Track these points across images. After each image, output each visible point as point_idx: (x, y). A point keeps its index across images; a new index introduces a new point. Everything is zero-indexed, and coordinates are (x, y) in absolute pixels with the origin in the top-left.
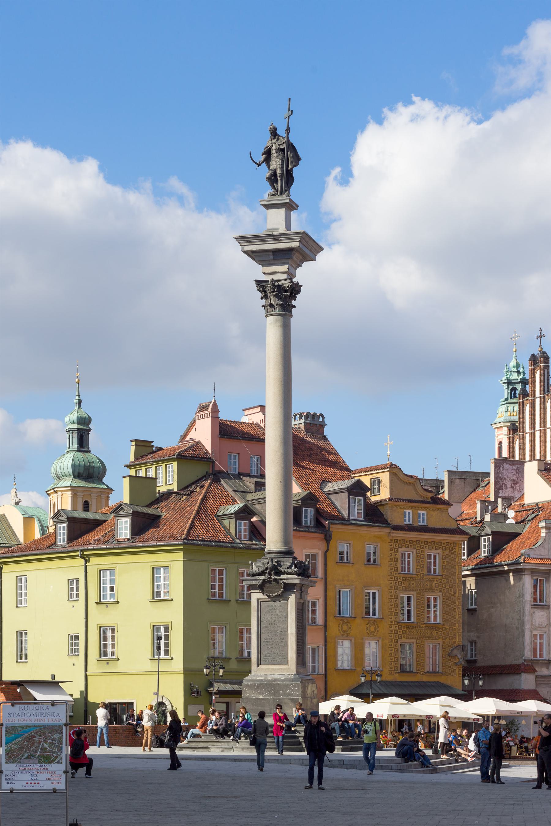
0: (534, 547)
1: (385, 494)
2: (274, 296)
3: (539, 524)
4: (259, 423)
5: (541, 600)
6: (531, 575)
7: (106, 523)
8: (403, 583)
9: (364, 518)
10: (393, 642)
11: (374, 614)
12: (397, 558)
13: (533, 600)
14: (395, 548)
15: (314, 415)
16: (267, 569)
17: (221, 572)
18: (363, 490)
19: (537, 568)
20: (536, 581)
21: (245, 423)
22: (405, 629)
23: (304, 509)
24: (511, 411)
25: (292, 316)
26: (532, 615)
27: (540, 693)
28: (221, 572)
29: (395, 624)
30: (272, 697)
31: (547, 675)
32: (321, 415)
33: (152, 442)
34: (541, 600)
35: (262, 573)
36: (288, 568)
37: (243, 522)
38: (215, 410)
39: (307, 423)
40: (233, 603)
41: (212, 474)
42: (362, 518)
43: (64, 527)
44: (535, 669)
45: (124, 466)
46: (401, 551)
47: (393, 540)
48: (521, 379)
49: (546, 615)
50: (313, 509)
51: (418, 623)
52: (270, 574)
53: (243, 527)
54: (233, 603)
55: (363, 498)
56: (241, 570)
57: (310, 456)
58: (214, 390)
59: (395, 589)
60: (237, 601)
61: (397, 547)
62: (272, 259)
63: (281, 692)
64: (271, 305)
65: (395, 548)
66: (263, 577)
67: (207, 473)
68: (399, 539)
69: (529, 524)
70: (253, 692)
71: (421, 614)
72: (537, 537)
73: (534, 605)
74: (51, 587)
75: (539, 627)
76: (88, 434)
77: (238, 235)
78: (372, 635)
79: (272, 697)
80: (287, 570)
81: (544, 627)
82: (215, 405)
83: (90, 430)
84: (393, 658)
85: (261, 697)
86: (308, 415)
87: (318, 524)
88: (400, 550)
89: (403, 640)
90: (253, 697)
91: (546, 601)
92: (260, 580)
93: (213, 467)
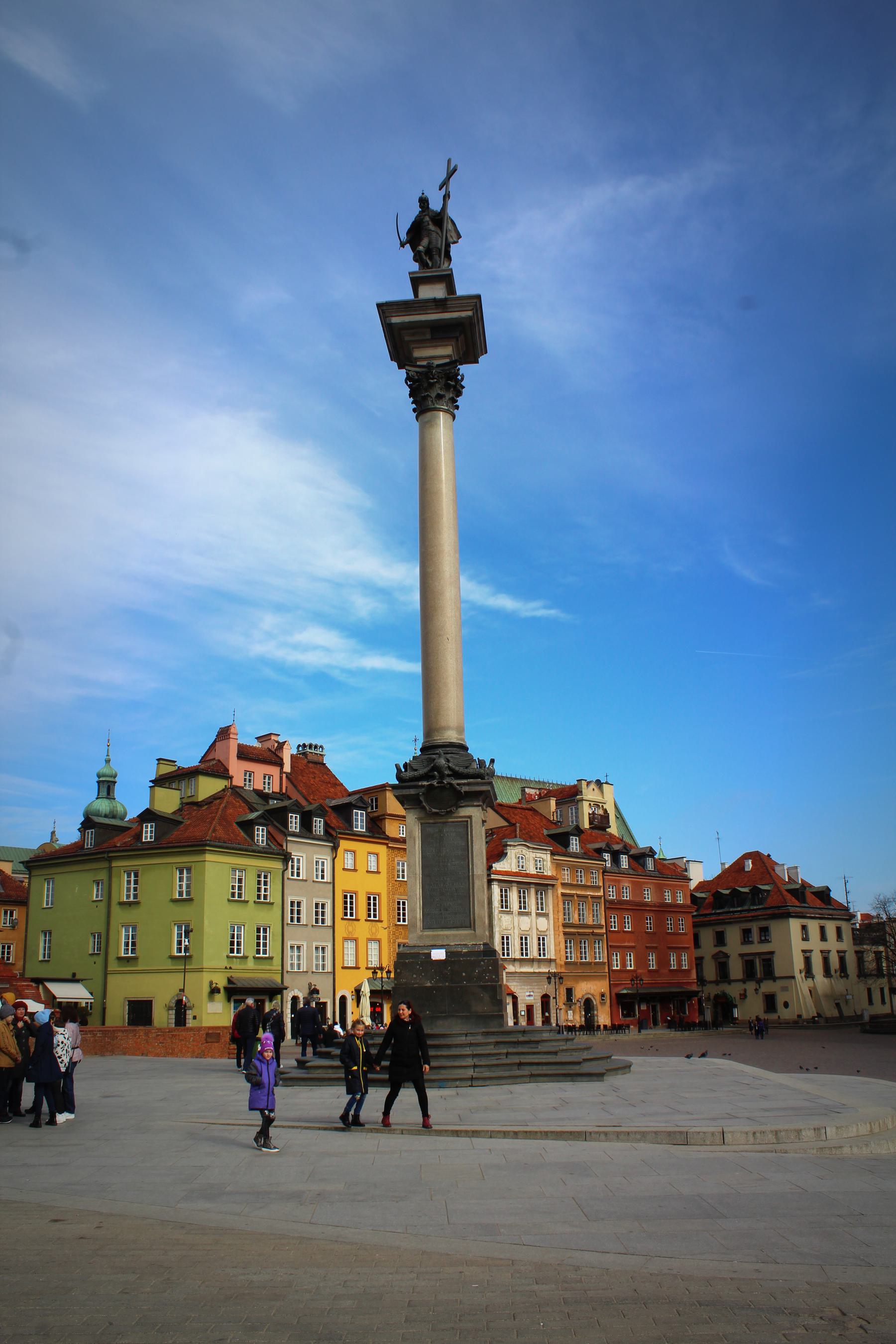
7: (131, 830)
10: (392, 942)
12: (394, 867)
13: (500, 906)
14: (392, 858)
15: (316, 747)
18: (364, 804)
19: (503, 879)
20: (501, 891)
22: (401, 930)
23: (314, 819)
26: (500, 919)
27: (510, 987)
30: (447, 984)
31: (514, 971)
32: (321, 747)
33: (176, 762)
36: (467, 767)
40: (251, 903)
41: (230, 788)
42: (364, 830)
43: (92, 832)
44: (505, 967)
45: (150, 781)
50: (322, 820)
54: (251, 903)
57: (314, 778)
60: (255, 902)
62: (428, 336)
63: (464, 974)
65: (392, 858)
66: (425, 783)
67: (226, 786)
70: (415, 976)
73: (501, 911)
74: (77, 888)
75: (505, 930)
76: (114, 785)
79: (447, 984)
80: (466, 771)
83: (115, 782)
84: (392, 957)
85: (429, 984)
88: (396, 860)
89: (400, 940)
90: (415, 984)
92: (423, 786)
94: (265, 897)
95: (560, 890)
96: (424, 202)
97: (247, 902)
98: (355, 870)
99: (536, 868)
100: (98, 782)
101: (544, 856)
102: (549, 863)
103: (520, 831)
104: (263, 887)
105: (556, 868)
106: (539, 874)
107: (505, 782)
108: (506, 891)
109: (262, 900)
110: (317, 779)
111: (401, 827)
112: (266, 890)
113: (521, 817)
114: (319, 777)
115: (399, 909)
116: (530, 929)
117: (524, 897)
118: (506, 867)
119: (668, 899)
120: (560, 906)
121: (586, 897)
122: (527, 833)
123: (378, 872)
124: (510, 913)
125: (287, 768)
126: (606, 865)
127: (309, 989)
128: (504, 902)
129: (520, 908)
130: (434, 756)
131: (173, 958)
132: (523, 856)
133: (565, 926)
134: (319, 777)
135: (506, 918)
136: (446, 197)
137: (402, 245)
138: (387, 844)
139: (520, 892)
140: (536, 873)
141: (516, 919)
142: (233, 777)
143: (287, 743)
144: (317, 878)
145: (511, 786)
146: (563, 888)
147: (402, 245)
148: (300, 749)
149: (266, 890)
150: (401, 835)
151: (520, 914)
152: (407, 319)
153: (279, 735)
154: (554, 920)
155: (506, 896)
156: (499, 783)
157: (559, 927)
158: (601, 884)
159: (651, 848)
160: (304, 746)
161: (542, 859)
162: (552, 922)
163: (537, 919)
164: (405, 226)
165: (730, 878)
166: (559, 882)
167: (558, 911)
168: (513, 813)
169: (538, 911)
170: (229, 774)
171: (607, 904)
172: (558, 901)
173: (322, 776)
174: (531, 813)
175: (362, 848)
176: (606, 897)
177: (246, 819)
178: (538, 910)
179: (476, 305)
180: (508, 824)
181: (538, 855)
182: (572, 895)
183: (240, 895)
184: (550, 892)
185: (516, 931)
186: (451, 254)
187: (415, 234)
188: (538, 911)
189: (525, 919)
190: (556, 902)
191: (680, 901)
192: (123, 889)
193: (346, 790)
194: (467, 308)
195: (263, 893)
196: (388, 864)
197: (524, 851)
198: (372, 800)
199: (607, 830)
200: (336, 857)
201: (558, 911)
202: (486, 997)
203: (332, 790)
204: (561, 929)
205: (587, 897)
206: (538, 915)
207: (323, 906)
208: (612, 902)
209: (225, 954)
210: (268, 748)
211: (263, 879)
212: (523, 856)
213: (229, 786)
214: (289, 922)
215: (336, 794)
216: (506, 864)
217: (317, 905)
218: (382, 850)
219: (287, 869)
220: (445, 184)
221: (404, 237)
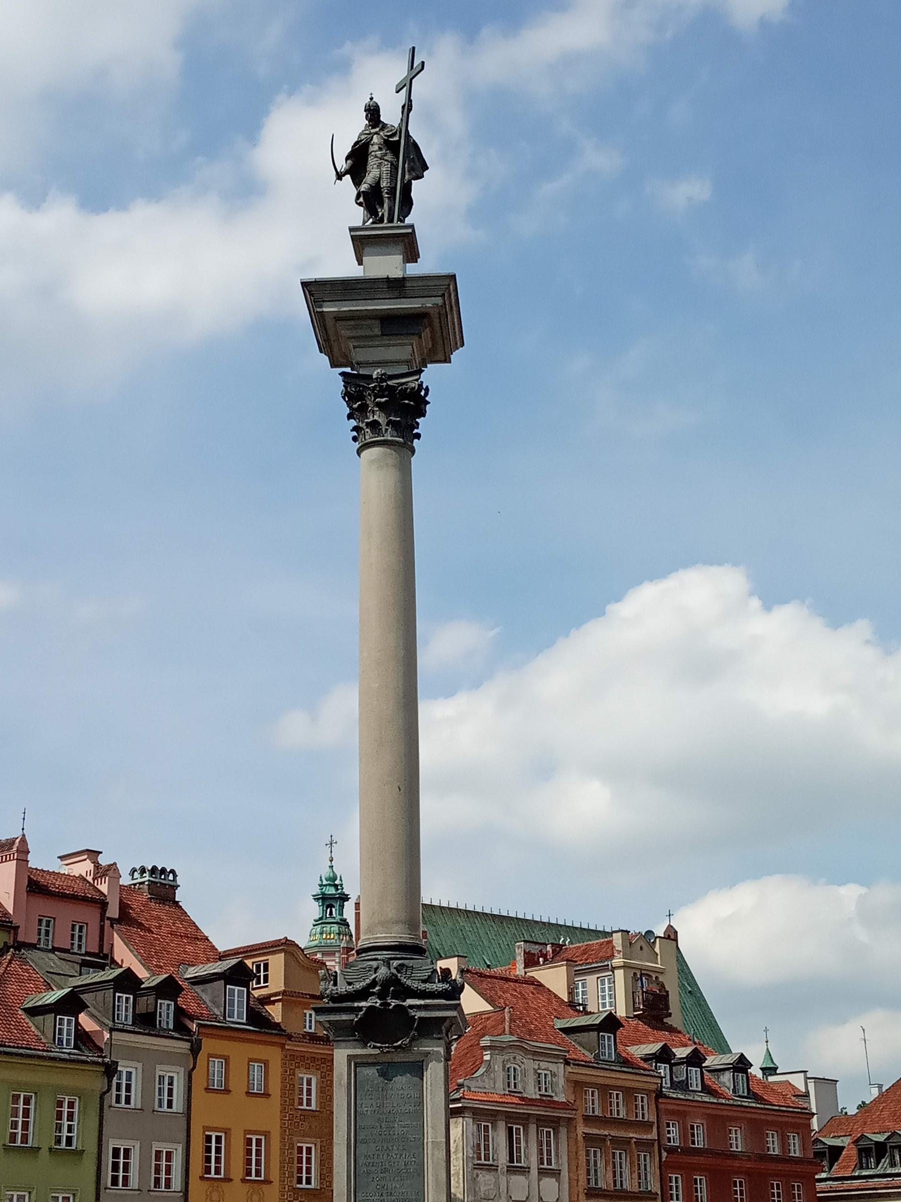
0: (474, 1076)
1: (276, 982)
2: (378, 405)
3: (481, 1042)
4: (85, 876)
5: (487, 1158)
6: (473, 1118)
8: (302, 1124)
9: (246, 1020)
13: (475, 1156)
14: (290, 1069)
15: (163, 871)
16: (374, 983)
17: (27, 1101)
21: (64, 874)
24: (327, 932)
25: (413, 451)
28: (27, 1101)
29: (289, 1191)
32: (172, 871)
34: (487, 1158)
35: (363, 994)
36: (424, 981)
37: (66, 1018)
38: (24, 851)
39: (152, 882)
40: (44, 1152)
42: (244, 1021)
47: (288, 1056)
48: (339, 894)
49: (494, 1180)
50: (173, 1003)
51: (323, 1190)
52: (382, 995)
53: (65, 1027)
54: (44, 1152)
55: (245, 989)
57: (160, 927)
58: (24, 819)
59: (290, 1135)
60: (50, 1149)
61: (293, 1068)
62: (377, 331)
64: (374, 425)
67: (5, 943)
68: (297, 1054)
69: (455, 1045)
71: (327, 1174)
72: (474, 1063)
73: (478, 1164)
80: (422, 986)
81: (492, 1199)
82: (23, 840)
86: (154, 870)
87: (181, 1028)
91: (493, 1158)
92: (360, 1009)
93: (16, 934)
94: (69, 1140)
95: (582, 1129)
97: (36, 1150)
98: (227, 1091)
99: (540, 1090)
101: (552, 1067)
102: (561, 1082)
103: (512, 1020)
104: (66, 1123)
105: (574, 1087)
106: (544, 1098)
107: (490, 924)
108: (486, 1127)
109: (63, 1145)
110: (164, 930)
111: (308, 1016)
114: (168, 926)
115: (300, 1160)
116: (527, 1198)
118: (487, 1087)
119: (774, 1148)
120: (580, 1158)
121: (628, 1141)
122: (524, 1026)
123: (266, 1095)
124: (492, 1168)
125: (113, 911)
126: (661, 1084)
129: (511, 1161)
130: (374, 964)
132: (518, 1067)
134: (168, 926)
136: (407, 108)
137: (339, 176)
138: (282, 1046)
139: (511, 1129)
140: (538, 1097)
141: (503, 1180)
142: (18, 927)
143: (114, 867)
144: (160, 1106)
145: (500, 930)
146: (586, 1126)
147: (339, 176)
148: (136, 875)
152: (346, 307)
153: (101, 853)
154: (570, 1183)
155: (486, 1138)
156: (478, 925)
157: (578, 1195)
158: (653, 1119)
159: (742, 1055)
160: (143, 870)
161: (549, 1072)
162: (566, 1186)
163: (539, 1180)
164: (344, 148)
165: (886, 1114)
166: (580, 1113)
167: (577, 1167)
168: (501, 989)
169: (542, 1166)
170: (11, 922)
171: (664, 1154)
172: (577, 1148)
173: (174, 924)
174: (531, 987)
175: (239, 1051)
176: (662, 1142)
177: (40, 1003)
178: (542, 1163)
179: (449, 288)
180: (490, 1008)
181: (543, 1065)
182: (602, 1139)
183: (25, 1138)
184: (563, 1131)
186: (412, 195)
188: (542, 1166)
189: (518, 1180)
190: (574, 1150)
191: (796, 1151)
193: (213, 948)
194: (435, 293)
195: (65, 1133)
196: (283, 1080)
197: (519, 1057)
198: (258, 967)
199: (665, 1020)
200: (194, 1068)
201: (577, 1167)
203: (189, 948)
205: (629, 1142)
206: (542, 1173)
207: (169, 1155)
208: (671, 1151)
210: (81, 875)
211: (65, 1109)
212: (518, 1067)
213: (12, 943)
215: (196, 957)
216: (487, 1080)
218: (274, 1055)
219: (109, 1090)
220: (406, 85)
221: (342, 165)
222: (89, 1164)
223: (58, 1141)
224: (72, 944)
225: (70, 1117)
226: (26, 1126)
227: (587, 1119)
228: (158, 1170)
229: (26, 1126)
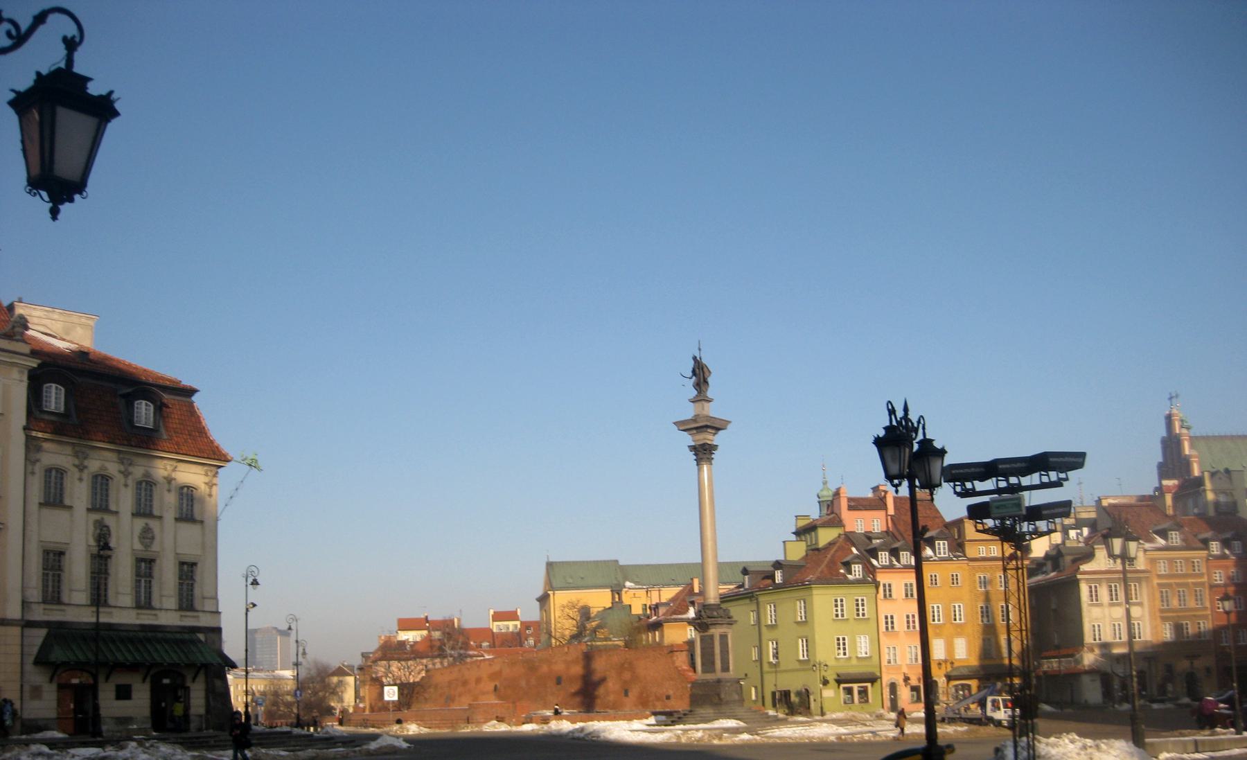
5: (1097, 600)
11: (960, 619)
20: (1091, 587)
34: (1097, 600)
40: (852, 621)
46: (977, 576)
54: (852, 621)
56: (856, 598)
77: (675, 421)
78: (959, 635)
93: (844, 528)
94: (863, 615)
95: (1156, 581)
96: (695, 358)
100: (819, 502)
104: (861, 608)
109: (861, 617)
112: (863, 610)
113: (1133, 516)
117: (1116, 590)
124: (1101, 605)
125: (891, 511)
127: (905, 676)
128: (1094, 595)
129: (1112, 600)
131: (800, 661)
133: (1162, 611)
135: (1096, 612)
141: (1106, 610)
149: (863, 610)
150: (981, 555)
151: (1112, 605)
155: (1096, 591)
158: (1204, 571)
183: (843, 615)
184: (1144, 585)
185: (1107, 620)
187: (694, 372)
192: (769, 615)
202: (717, 698)
204: (1158, 614)
209: (833, 657)
214: (884, 630)
217: (908, 617)
221: (690, 374)
222: (873, 624)
223: (858, 615)
224: (874, 529)
225: (863, 605)
226: (842, 610)
227: (1160, 576)
228: (908, 622)
229: (842, 610)
